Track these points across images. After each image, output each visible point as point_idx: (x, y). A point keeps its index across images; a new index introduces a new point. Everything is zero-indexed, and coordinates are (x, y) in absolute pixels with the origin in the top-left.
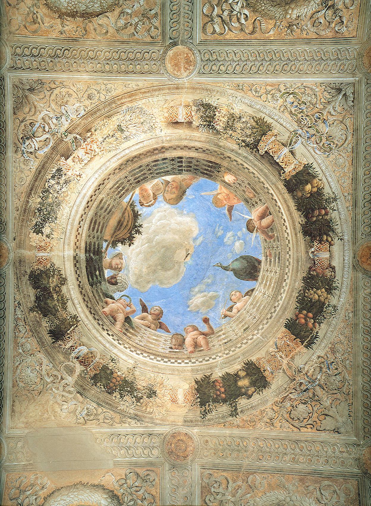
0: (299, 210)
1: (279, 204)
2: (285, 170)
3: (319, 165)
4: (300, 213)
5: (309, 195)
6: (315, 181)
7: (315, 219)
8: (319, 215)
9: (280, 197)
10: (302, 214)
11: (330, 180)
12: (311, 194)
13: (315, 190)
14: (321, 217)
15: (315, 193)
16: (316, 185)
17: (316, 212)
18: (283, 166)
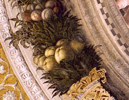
0: (75, 19)
1: (108, 28)
2: (99, 84)
3: (43, 93)
4: (72, 14)
5: (58, 44)
6: (48, 67)
7: (48, 4)
8: (41, 10)
9: (106, 39)
10: (68, 13)
11: (24, 70)
12: (54, 45)
13: (48, 53)
14: (37, 7)
15: (48, 47)
16: (47, 60)
17: (45, 15)
18: (102, 90)
